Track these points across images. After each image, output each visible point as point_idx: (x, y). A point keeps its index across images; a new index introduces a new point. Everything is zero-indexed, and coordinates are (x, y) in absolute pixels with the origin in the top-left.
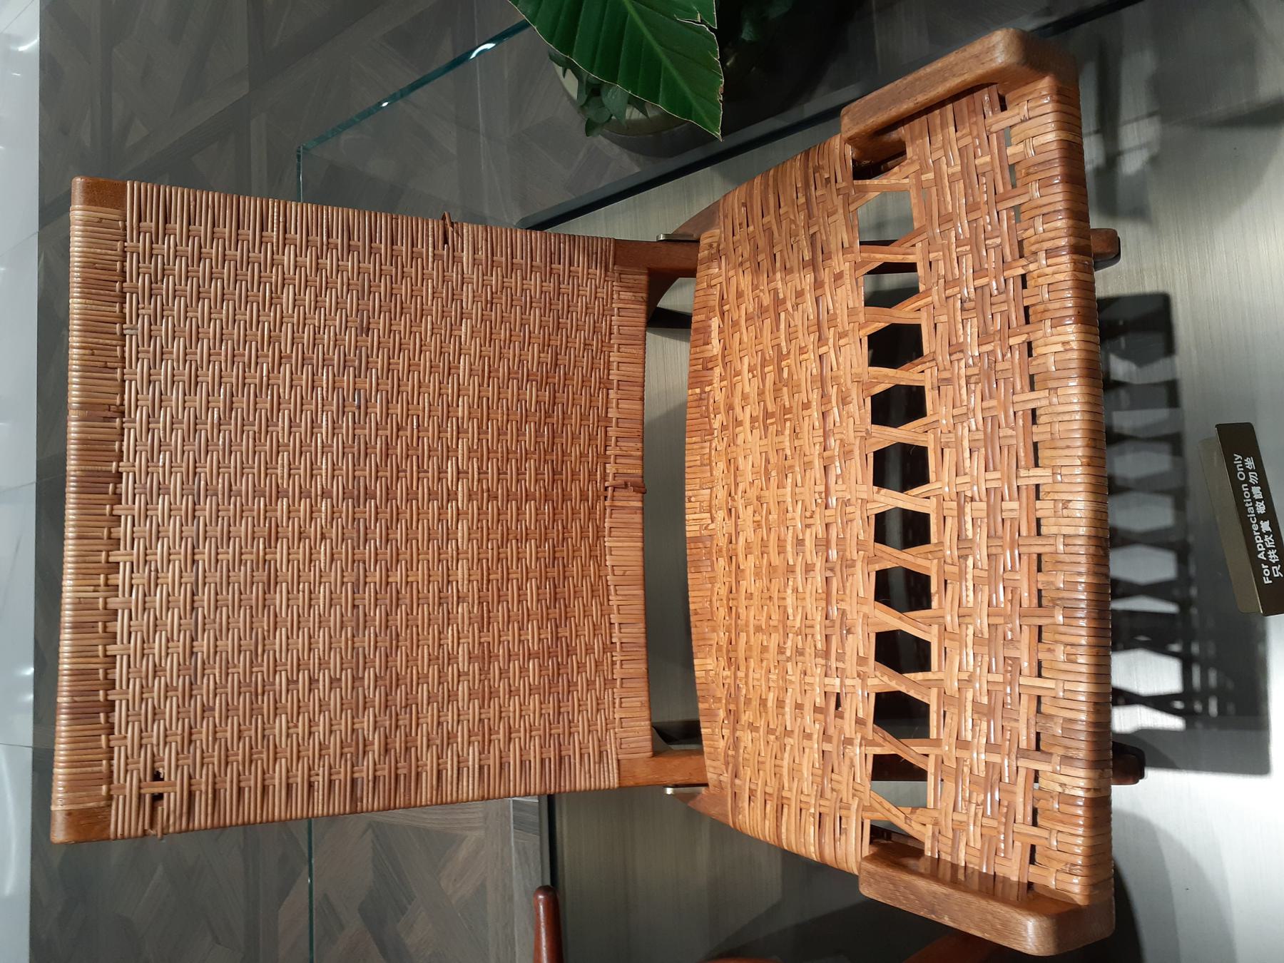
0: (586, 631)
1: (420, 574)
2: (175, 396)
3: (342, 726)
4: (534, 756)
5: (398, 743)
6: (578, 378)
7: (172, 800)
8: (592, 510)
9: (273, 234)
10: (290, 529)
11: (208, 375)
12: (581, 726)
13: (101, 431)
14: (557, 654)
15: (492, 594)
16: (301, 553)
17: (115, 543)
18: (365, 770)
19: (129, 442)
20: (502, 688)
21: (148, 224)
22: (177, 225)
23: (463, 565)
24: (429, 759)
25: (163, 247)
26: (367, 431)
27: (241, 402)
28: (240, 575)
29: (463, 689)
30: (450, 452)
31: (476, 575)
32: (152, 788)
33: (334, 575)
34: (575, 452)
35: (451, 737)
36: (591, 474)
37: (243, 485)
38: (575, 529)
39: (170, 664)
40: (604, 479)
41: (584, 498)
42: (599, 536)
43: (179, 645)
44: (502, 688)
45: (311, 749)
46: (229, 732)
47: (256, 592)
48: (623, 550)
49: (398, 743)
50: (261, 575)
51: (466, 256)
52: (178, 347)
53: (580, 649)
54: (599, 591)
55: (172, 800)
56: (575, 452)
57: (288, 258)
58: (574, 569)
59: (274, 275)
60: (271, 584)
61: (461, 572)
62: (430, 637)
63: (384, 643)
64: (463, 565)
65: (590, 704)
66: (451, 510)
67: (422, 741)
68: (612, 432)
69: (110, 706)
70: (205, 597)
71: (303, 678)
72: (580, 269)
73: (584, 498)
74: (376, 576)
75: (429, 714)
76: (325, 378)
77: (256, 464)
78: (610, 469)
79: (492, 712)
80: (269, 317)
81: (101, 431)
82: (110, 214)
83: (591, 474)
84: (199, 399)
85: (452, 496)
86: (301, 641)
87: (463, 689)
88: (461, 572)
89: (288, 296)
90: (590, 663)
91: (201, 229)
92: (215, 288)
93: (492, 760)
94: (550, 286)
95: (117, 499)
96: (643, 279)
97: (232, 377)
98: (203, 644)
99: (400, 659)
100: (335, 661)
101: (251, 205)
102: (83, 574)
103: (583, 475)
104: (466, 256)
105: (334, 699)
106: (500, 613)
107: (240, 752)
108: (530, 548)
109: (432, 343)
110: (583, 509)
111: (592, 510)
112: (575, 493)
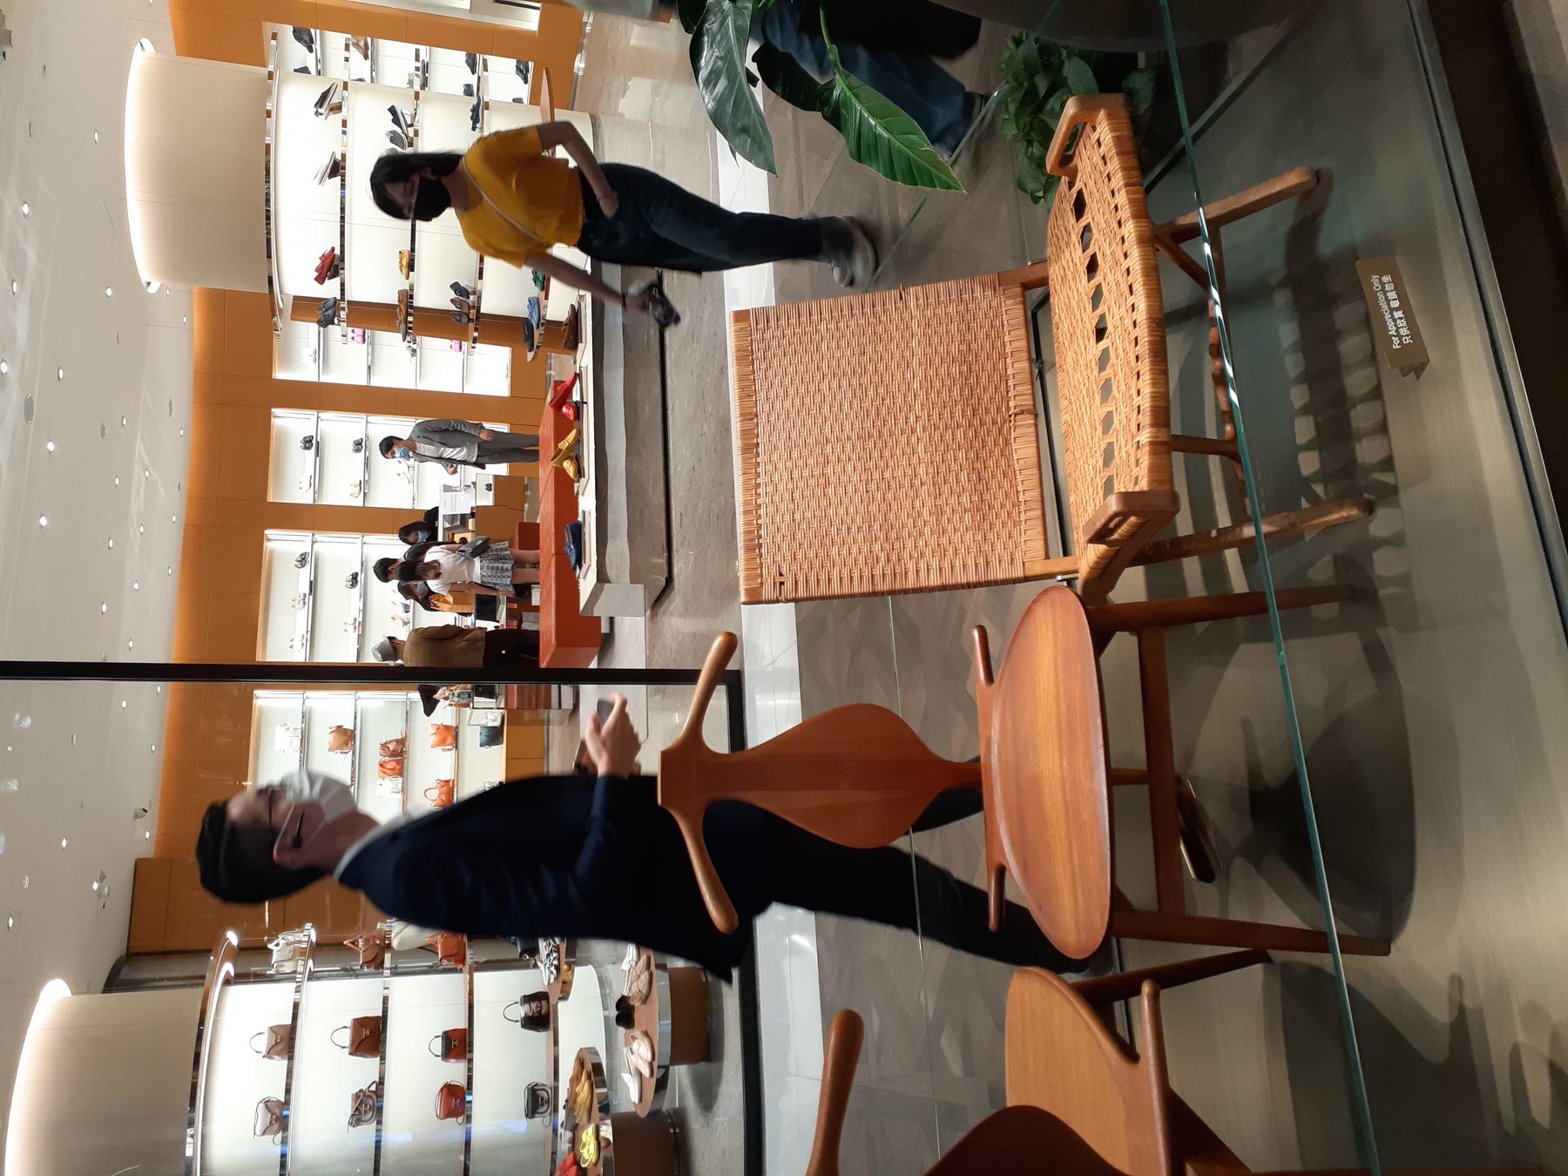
0: (1001, 496)
1: (899, 473)
2: (778, 405)
3: (865, 549)
4: (970, 562)
5: (894, 557)
6: (983, 355)
7: (789, 585)
8: (1000, 431)
9: (815, 317)
10: (833, 458)
11: (791, 391)
12: (999, 546)
13: (749, 425)
14: (982, 511)
15: (940, 480)
16: (839, 469)
17: (758, 475)
18: (878, 571)
19: (760, 430)
20: (950, 528)
21: (761, 326)
22: (772, 323)
23: (923, 466)
24: (911, 565)
25: (767, 335)
26: (866, 404)
27: (807, 401)
28: (812, 482)
29: (927, 530)
30: (910, 408)
31: (931, 470)
32: (779, 579)
33: (855, 478)
34: (986, 397)
35: (922, 555)
36: (998, 410)
37: (810, 441)
38: (990, 441)
39: (784, 527)
40: (1008, 409)
41: (994, 422)
42: (1007, 443)
43: (788, 517)
44: (950, 528)
45: (850, 561)
46: (811, 554)
47: (819, 492)
48: (1024, 450)
49: (894, 557)
50: (822, 481)
51: (912, 304)
52: (777, 382)
53: (997, 505)
54: (1009, 473)
55: (789, 585)
56: (986, 397)
57: (822, 327)
58: (991, 463)
59: (817, 338)
60: (827, 484)
61: (921, 470)
62: (907, 504)
63: (884, 507)
64: (923, 466)
65: (1004, 534)
66: (914, 440)
67: (906, 555)
68: (1011, 383)
69: (760, 546)
70: (797, 495)
71: (844, 528)
72: (978, 294)
73: (994, 422)
74: (876, 476)
75: (910, 544)
76: (844, 383)
77: (816, 431)
78: (1012, 404)
79: (944, 540)
80: (817, 357)
81: (749, 425)
82: (744, 325)
83: (998, 410)
84: (788, 404)
85: (913, 431)
86: (842, 511)
87: (927, 530)
88: (921, 470)
89: (824, 346)
90: (1004, 514)
91: (783, 322)
92: (790, 350)
93: (946, 565)
94: (961, 308)
95: (758, 455)
96: (1019, 290)
97: (802, 390)
98: (798, 516)
99: (892, 516)
100: (859, 519)
101: (804, 307)
102: (746, 490)
103: (993, 409)
104: (912, 304)
105: (860, 538)
106: (946, 490)
107: (817, 564)
108: (961, 455)
109: (897, 354)
110: (995, 430)
111: (1000, 431)
112: (988, 419)
